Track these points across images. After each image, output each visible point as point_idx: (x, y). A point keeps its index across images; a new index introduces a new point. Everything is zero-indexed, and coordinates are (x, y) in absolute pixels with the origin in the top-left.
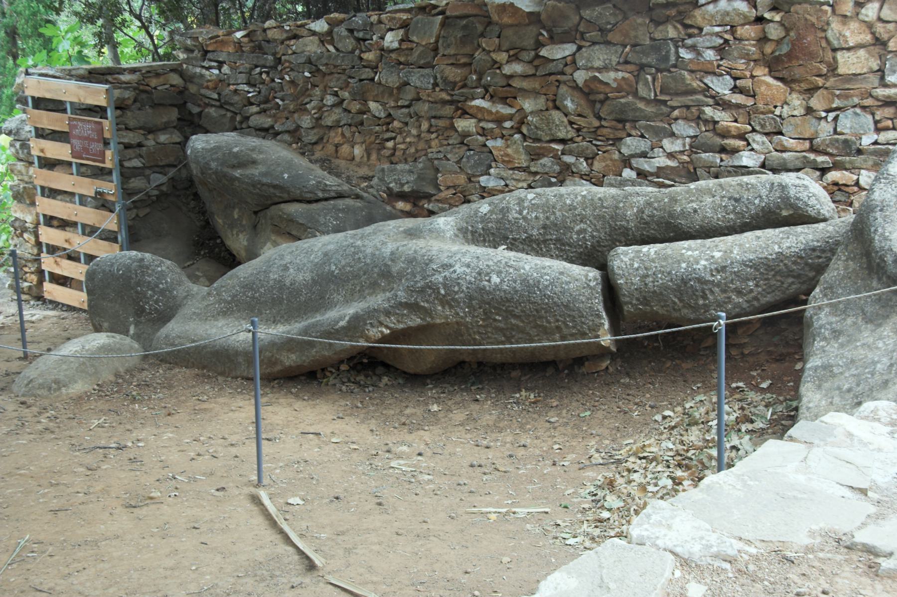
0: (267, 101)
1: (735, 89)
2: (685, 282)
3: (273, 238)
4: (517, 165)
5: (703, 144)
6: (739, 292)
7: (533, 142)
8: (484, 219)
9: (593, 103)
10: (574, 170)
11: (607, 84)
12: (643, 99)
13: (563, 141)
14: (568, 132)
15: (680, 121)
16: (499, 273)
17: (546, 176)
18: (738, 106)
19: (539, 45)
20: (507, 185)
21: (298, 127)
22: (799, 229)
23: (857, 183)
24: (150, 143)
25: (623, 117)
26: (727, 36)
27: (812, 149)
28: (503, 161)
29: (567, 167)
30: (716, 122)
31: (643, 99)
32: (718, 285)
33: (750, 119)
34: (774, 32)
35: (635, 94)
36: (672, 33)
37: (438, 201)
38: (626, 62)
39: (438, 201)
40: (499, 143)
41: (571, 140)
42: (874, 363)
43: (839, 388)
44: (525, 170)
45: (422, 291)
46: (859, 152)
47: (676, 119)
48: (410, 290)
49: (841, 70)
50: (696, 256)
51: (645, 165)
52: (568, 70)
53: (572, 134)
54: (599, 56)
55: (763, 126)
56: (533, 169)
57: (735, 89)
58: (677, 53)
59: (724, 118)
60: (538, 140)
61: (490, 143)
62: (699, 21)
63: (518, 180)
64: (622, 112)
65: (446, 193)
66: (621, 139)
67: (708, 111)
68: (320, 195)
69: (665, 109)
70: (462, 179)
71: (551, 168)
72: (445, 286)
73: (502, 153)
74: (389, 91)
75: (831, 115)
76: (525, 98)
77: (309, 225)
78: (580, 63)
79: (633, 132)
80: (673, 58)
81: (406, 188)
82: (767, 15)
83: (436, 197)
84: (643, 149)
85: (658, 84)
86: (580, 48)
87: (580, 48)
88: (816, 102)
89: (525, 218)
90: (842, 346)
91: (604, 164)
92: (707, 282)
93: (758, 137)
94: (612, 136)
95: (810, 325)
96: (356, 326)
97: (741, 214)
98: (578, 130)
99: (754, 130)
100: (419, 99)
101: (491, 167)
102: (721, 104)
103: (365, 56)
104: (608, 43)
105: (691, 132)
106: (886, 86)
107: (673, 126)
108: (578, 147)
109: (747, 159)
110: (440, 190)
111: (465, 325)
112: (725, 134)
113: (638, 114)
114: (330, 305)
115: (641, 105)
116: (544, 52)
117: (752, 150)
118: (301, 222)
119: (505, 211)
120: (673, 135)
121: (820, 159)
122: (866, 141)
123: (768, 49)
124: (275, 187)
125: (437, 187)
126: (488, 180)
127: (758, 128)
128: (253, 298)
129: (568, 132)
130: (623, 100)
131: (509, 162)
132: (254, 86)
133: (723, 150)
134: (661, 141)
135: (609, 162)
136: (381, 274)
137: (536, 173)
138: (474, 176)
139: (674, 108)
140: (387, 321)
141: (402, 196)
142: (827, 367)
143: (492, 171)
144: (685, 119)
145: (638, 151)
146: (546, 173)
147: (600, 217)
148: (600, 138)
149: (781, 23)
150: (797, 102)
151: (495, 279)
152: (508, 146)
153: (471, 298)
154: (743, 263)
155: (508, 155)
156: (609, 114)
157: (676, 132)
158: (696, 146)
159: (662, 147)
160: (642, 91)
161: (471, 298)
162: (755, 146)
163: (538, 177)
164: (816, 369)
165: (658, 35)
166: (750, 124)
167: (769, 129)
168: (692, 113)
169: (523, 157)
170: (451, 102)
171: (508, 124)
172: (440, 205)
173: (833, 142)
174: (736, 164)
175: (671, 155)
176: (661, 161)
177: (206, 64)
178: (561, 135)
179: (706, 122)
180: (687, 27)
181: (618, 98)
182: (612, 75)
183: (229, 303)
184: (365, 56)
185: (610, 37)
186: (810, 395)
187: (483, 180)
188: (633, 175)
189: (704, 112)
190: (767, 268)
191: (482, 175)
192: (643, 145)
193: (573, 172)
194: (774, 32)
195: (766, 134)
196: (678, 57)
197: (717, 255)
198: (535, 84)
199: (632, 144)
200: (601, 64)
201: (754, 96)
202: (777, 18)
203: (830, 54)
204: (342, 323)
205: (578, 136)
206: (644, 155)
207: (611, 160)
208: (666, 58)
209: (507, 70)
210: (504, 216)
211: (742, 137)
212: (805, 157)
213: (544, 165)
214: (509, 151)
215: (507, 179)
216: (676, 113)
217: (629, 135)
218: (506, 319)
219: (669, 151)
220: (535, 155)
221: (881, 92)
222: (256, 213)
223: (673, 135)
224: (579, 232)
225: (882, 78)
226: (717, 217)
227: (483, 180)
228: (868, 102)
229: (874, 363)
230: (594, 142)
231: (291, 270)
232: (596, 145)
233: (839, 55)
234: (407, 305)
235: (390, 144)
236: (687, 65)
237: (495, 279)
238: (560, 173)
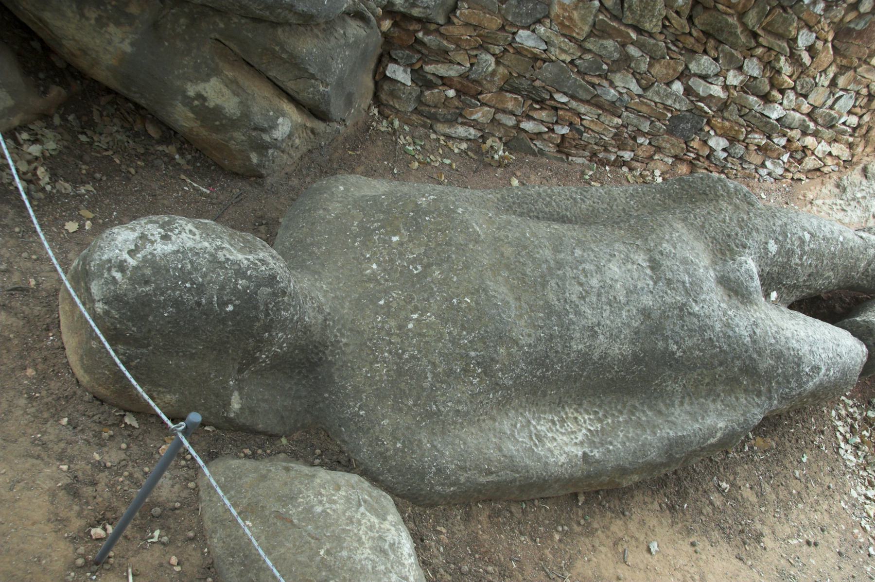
1: (810, 49)
3: (230, 74)
4: (574, 35)
5: (756, 87)
7: (610, 19)
10: (633, 65)
12: (744, 25)
13: (639, 30)
14: (656, 25)
15: (755, 60)
17: (599, 59)
20: (545, 51)
25: (716, 34)
28: (561, 24)
31: (744, 25)
33: (799, 78)
35: (741, 15)
37: (441, 34)
39: (441, 34)
41: (651, 35)
47: (752, 56)
51: (701, 87)
55: (803, 87)
56: (588, 45)
57: (810, 49)
63: (563, 51)
64: (721, 30)
65: (462, 30)
66: (696, 52)
67: (783, 58)
69: (753, 44)
70: (493, 23)
71: (611, 53)
73: (566, 14)
77: (319, 76)
79: (713, 53)
83: (442, 30)
84: (709, 72)
88: (841, 81)
91: (665, 71)
93: (792, 95)
94: (690, 47)
98: (664, 26)
99: (794, 89)
101: (539, 21)
102: (794, 58)
105: (756, 73)
107: (746, 61)
108: (654, 45)
110: (449, 22)
113: (730, 39)
117: (781, 104)
118: (312, 71)
120: (740, 69)
121: (812, 125)
126: (529, 36)
127: (799, 88)
128: (543, 377)
129: (656, 25)
130: (730, 20)
131: (568, 27)
133: (766, 98)
134: (728, 70)
135: (671, 72)
137: (589, 51)
138: (512, 25)
139: (759, 45)
143: (541, 29)
144: (760, 59)
145: (704, 73)
146: (600, 56)
148: (681, 45)
152: (576, 8)
155: (570, 19)
156: (703, 24)
157: (745, 68)
158: (748, 87)
159: (725, 78)
160: (751, 19)
162: (785, 102)
163: (588, 57)
166: (795, 82)
167: (803, 92)
168: (770, 56)
169: (587, 29)
172: (445, 43)
174: (765, 113)
175: (726, 87)
176: (716, 90)
178: (648, 26)
181: (726, 13)
183: (508, 388)
189: (779, 60)
191: (523, 28)
193: (629, 67)
195: (796, 93)
199: (704, 63)
201: (812, 58)
204: (712, 441)
205: (661, 33)
206: (705, 78)
207: (674, 70)
210: (788, 260)
212: (804, 121)
213: (605, 48)
214: (576, 15)
215: (553, 45)
216: (760, 51)
217: (705, 52)
219: (728, 83)
220: (599, 31)
223: (740, 69)
227: (524, 38)
230: (670, 45)
231: (601, 337)
232: (668, 48)
236: (802, 12)
238: (614, 61)
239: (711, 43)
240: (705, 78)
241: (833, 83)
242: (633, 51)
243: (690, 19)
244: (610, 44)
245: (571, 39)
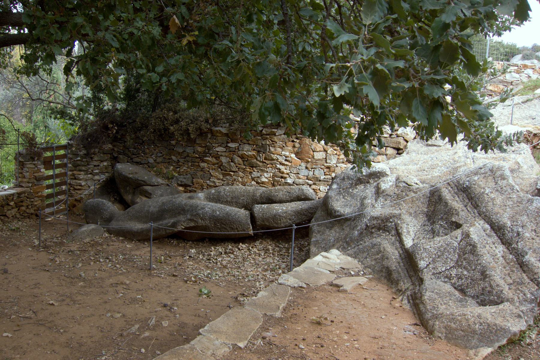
0: (139, 154)
2: (275, 216)
3: (140, 196)
6: (290, 220)
8: (213, 194)
9: (243, 161)
11: (248, 156)
16: (219, 211)
18: (287, 165)
19: (228, 143)
21: (149, 162)
22: (307, 202)
23: (319, 190)
24: (102, 165)
26: (284, 145)
27: (307, 179)
29: (235, 180)
30: (280, 169)
32: (284, 217)
34: (297, 145)
36: (268, 143)
38: (254, 150)
40: (214, 171)
42: (330, 240)
43: (321, 247)
44: (222, 180)
45: (195, 215)
46: (320, 181)
48: (192, 215)
49: (315, 158)
50: (278, 208)
52: (237, 150)
53: (237, 170)
54: (247, 147)
57: (286, 160)
58: (269, 149)
59: (282, 168)
60: (226, 171)
61: (210, 171)
62: (276, 140)
68: (156, 184)
72: (202, 214)
74: (179, 153)
75: (313, 170)
76: (223, 158)
78: (240, 149)
80: (268, 150)
81: (183, 183)
82: (295, 140)
85: (263, 157)
86: (240, 145)
87: (240, 145)
88: (309, 166)
89: (226, 195)
90: (321, 235)
92: (281, 216)
93: (292, 174)
95: (311, 229)
96: (174, 225)
97: (290, 197)
100: (188, 156)
103: (172, 142)
104: (249, 144)
106: (327, 163)
109: (289, 181)
111: (208, 226)
112: (283, 173)
114: (165, 219)
115: (259, 163)
116: (229, 145)
119: (219, 192)
122: (322, 178)
123: (296, 149)
124: (142, 181)
125: (193, 183)
132: (135, 149)
133: (282, 177)
136: (181, 210)
140: (183, 224)
141: (181, 185)
142: (317, 241)
147: (248, 196)
149: (299, 143)
150: (303, 165)
151: (218, 213)
153: (210, 218)
154: (291, 211)
158: (274, 176)
160: (259, 158)
161: (210, 218)
164: (314, 241)
165: (263, 143)
170: (199, 158)
171: (217, 165)
173: (314, 178)
175: (266, 178)
177: (120, 142)
178: (234, 170)
179: (277, 169)
180: (272, 141)
182: (250, 153)
184: (172, 142)
185: (250, 142)
186: (313, 249)
187: (208, 181)
188: (255, 183)
190: (298, 213)
192: (259, 175)
194: (297, 145)
196: (270, 149)
197: (284, 208)
198: (227, 154)
200: (248, 150)
202: (298, 141)
203: (312, 153)
208: (266, 150)
209: (217, 149)
211: (288, 174)
214: (217, 174)
216: (268, 166)
218: (221, 225)
221: (326, 164)
222: (134, 189)
224: (242, 200)
225: (326, 161)
226: (284, 198)
228: (323, 167)
229: (330, 240)
233: (315, 153)
234: (190, 220)
235: (178, 169)
237: (218, 213)
239: (254, 168)
240: (258, 177)
241: (307, 168)
242: (234, 177)
243: (245, 165)
244: (228, 177)
245: (219, 179)
